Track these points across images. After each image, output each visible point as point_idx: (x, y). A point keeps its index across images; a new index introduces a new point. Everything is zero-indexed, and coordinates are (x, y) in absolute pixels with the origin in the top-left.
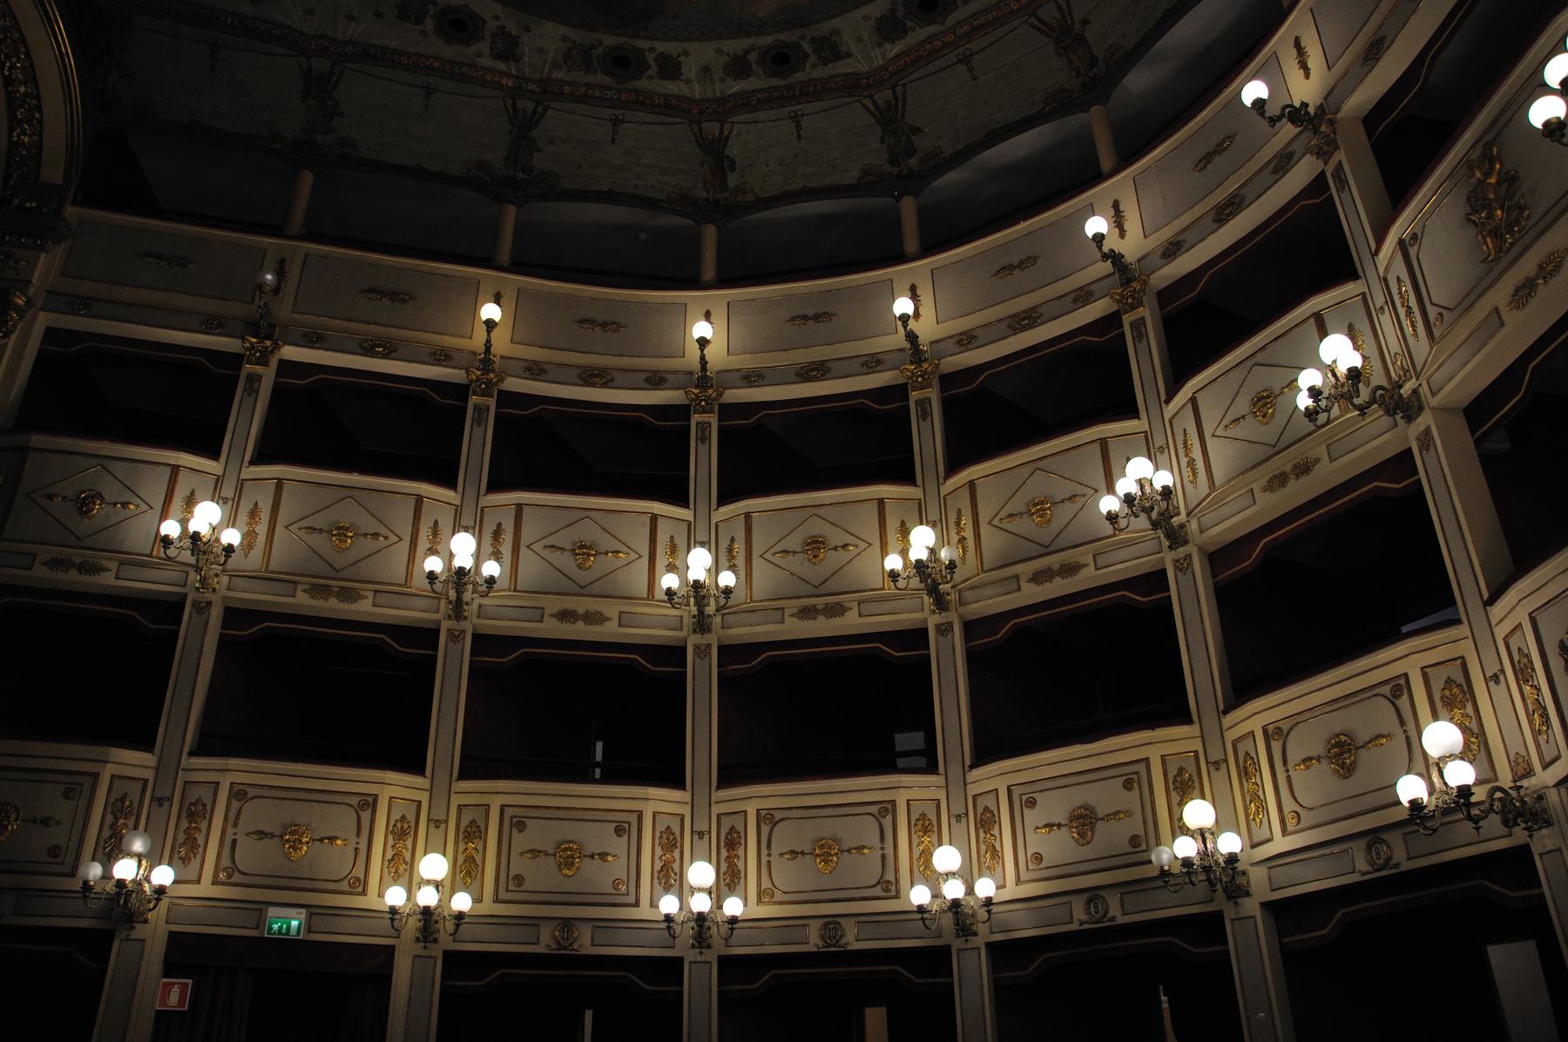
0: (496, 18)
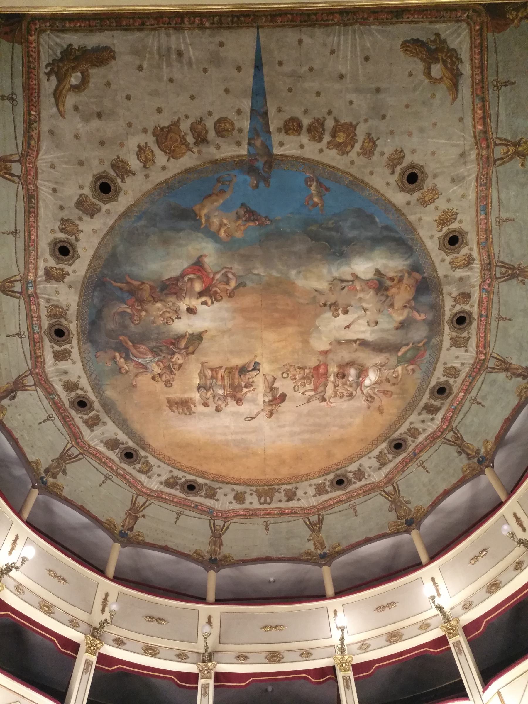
0: (74, 272)
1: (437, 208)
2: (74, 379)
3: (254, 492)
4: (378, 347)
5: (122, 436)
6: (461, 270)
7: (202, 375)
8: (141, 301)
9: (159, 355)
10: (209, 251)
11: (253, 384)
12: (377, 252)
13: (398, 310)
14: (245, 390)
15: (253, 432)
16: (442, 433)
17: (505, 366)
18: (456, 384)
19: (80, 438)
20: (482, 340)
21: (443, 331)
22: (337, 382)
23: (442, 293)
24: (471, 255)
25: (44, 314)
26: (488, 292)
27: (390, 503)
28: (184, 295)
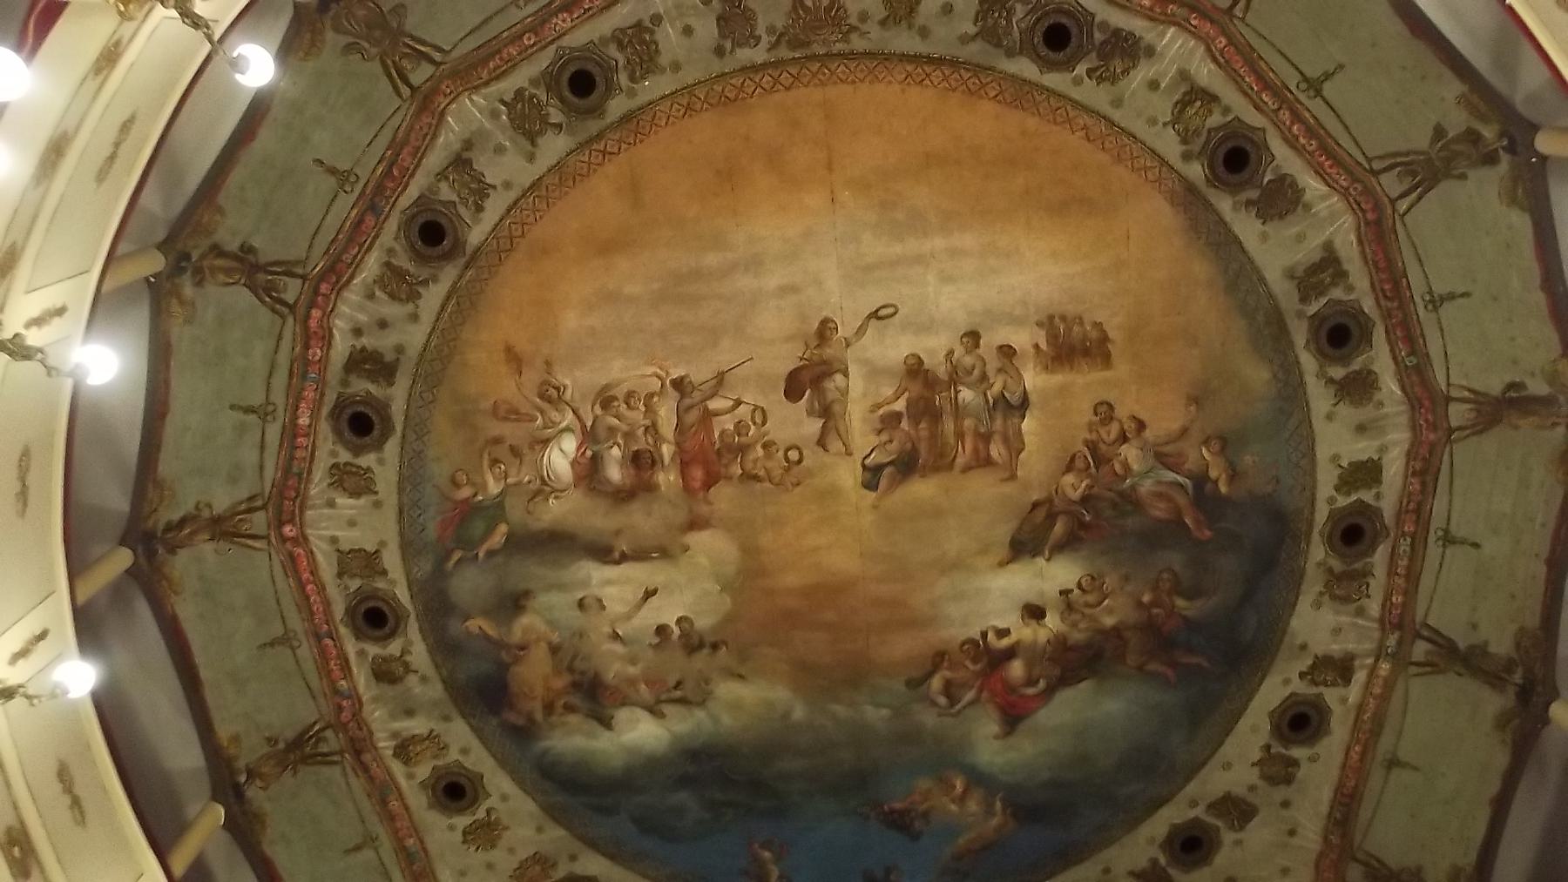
0: (1287, 682)
1: (511, 851)
2: (1345, 410)
3: (853, 29)
4: (559, 544)
5: (1247, 228)
6: (417, 732)
7: (1015, 445)
8: (1150, 628)
9: (1121, 494)
10: (988, 745)
11: (879, 426)
12: (618, 762)
13: (538, 640)
14: (900, 405)
15: (869, 268)
16: (316, 292)
17: (223, 528)
18: (328, 450)
19: (1367, 223)
20: (306, 575)
21: (410, 589)
22: (650, 440)
23: (444, 682)
24: (406, 763)
25: (1377, 584)
26: (337, 692)
27: (408, 28)
28: (1049, 649)
